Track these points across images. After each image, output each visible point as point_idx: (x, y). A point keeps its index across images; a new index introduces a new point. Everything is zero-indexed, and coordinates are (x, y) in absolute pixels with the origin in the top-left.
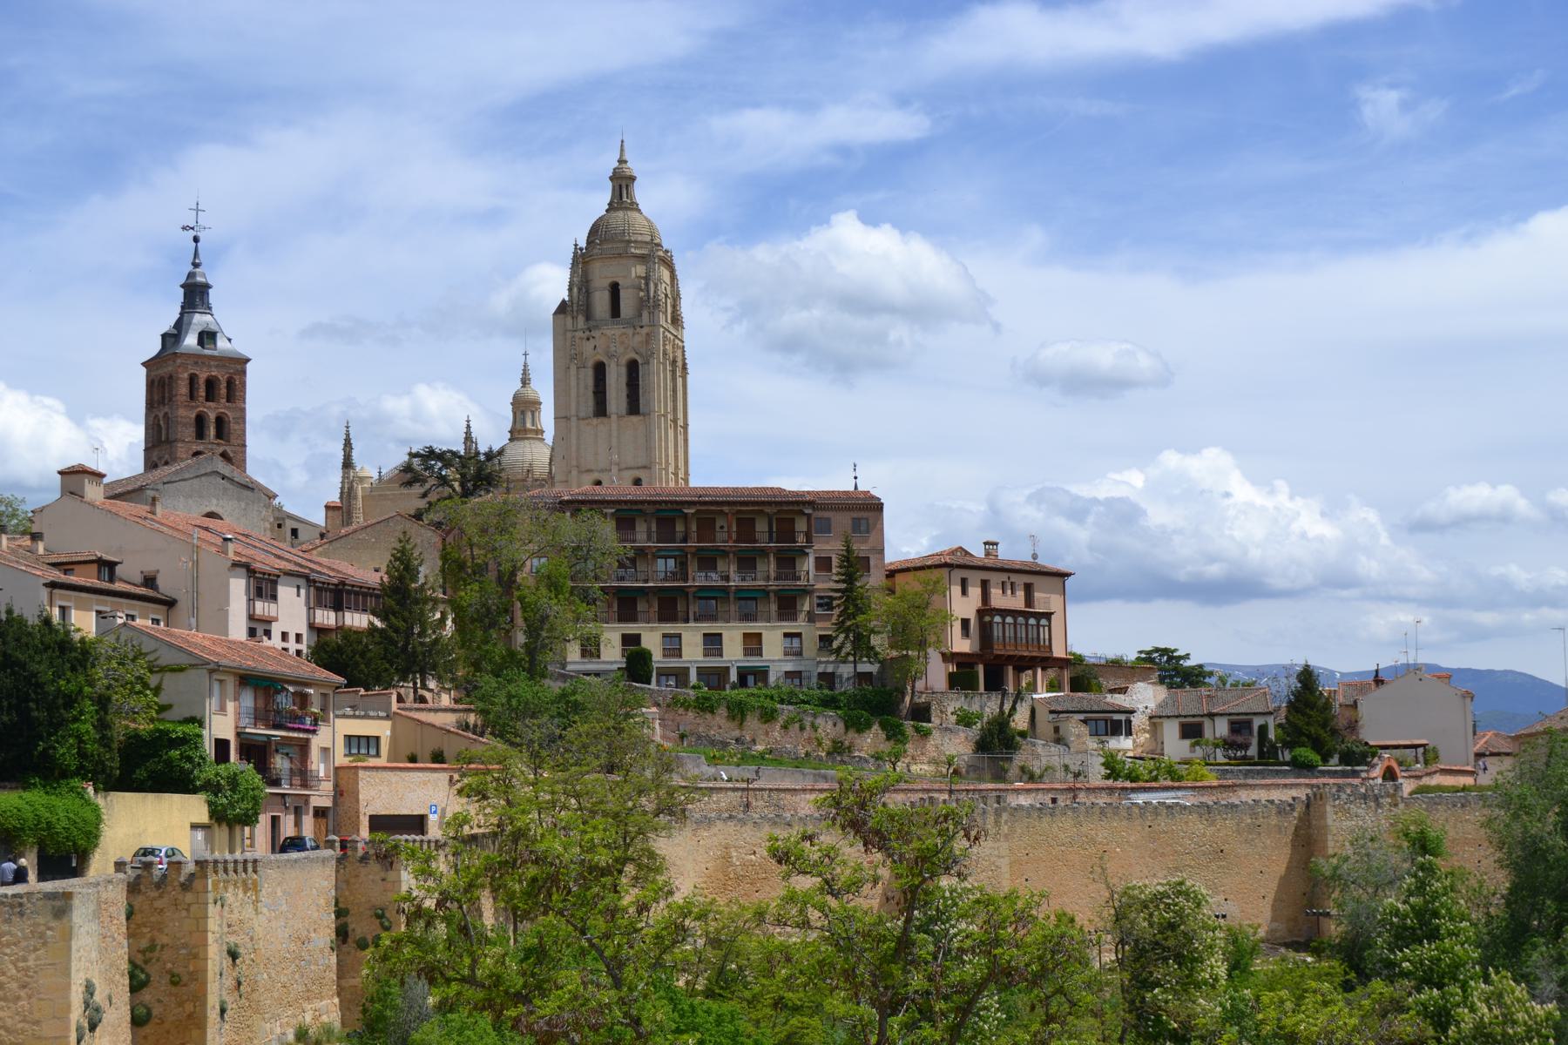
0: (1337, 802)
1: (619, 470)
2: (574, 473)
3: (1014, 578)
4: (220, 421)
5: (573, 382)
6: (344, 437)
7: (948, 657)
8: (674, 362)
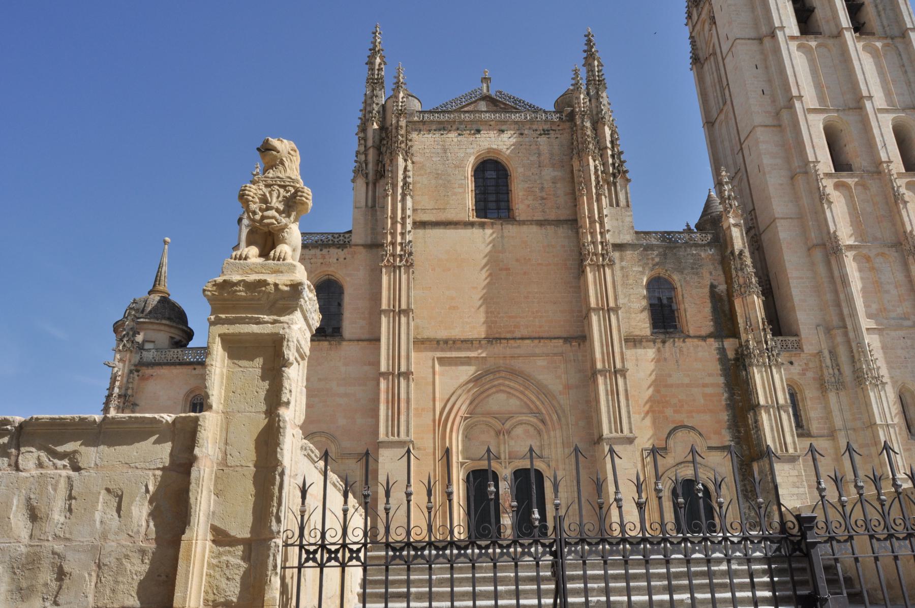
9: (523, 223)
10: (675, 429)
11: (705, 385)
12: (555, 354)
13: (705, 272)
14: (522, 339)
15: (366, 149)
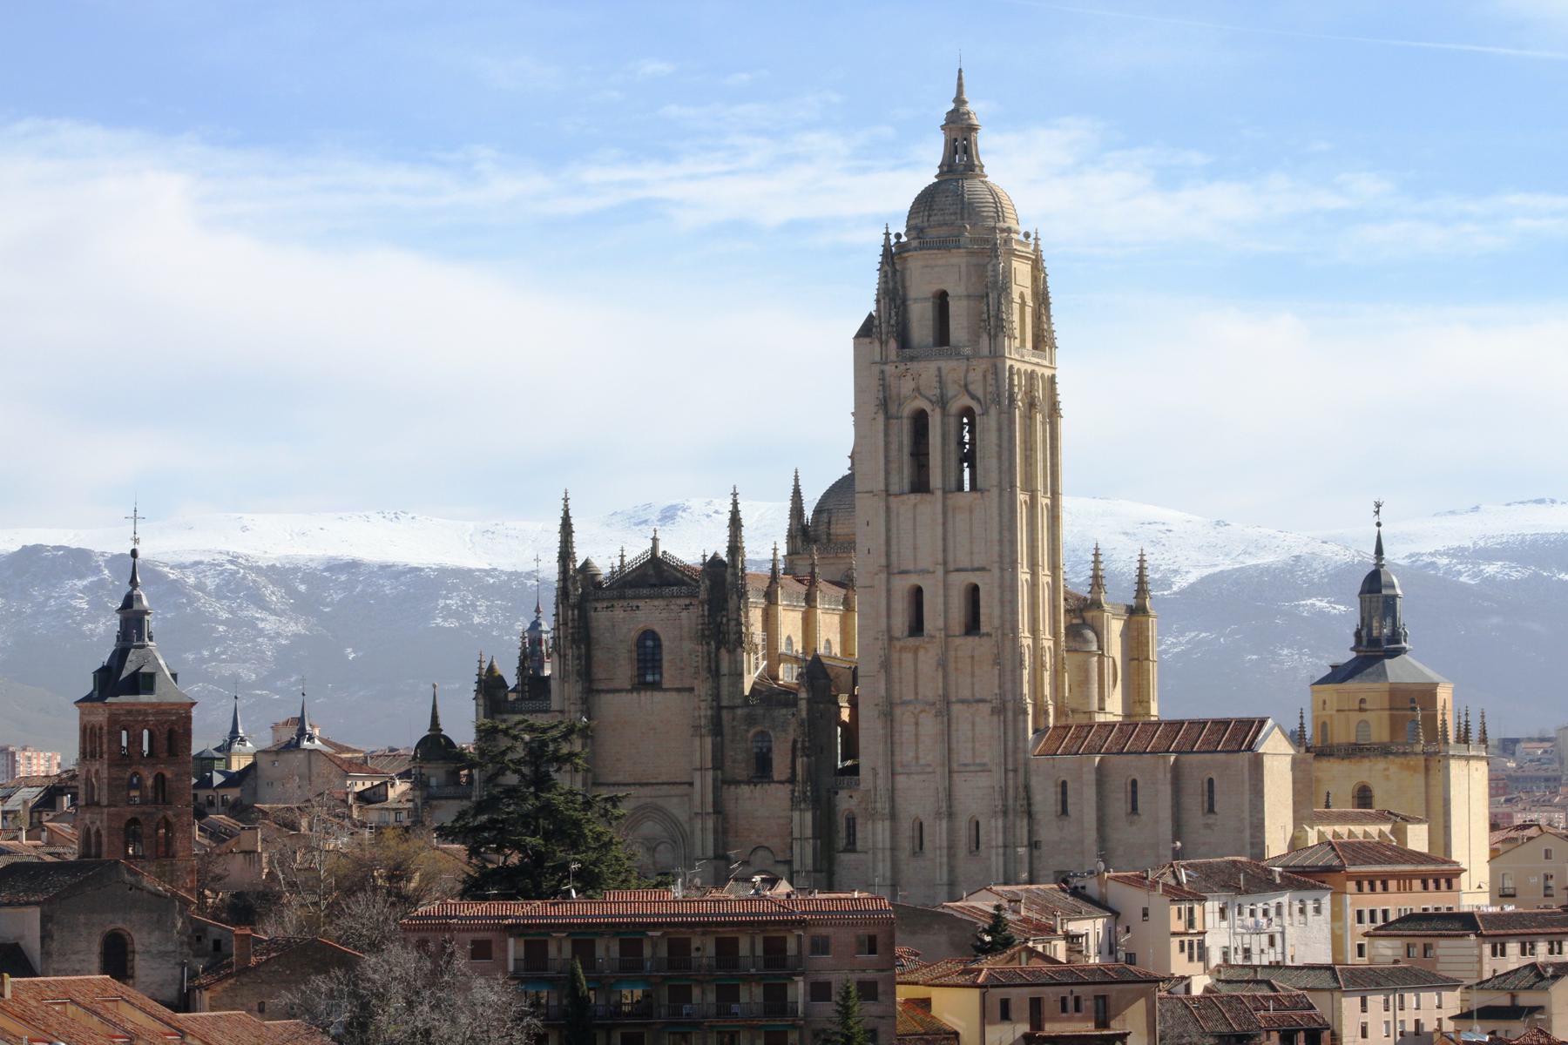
1: (946, 572)
2: (883, 576)
3: (1077, 990)
4: (160, 779)
5: (881, 435)
6: (562, 514)
8: (1032, 405)
10: (755, 849)
11: (779, 817)
12: (682, 796)
13: (791, 730)
14: (663, 784)
15: (559, 625)
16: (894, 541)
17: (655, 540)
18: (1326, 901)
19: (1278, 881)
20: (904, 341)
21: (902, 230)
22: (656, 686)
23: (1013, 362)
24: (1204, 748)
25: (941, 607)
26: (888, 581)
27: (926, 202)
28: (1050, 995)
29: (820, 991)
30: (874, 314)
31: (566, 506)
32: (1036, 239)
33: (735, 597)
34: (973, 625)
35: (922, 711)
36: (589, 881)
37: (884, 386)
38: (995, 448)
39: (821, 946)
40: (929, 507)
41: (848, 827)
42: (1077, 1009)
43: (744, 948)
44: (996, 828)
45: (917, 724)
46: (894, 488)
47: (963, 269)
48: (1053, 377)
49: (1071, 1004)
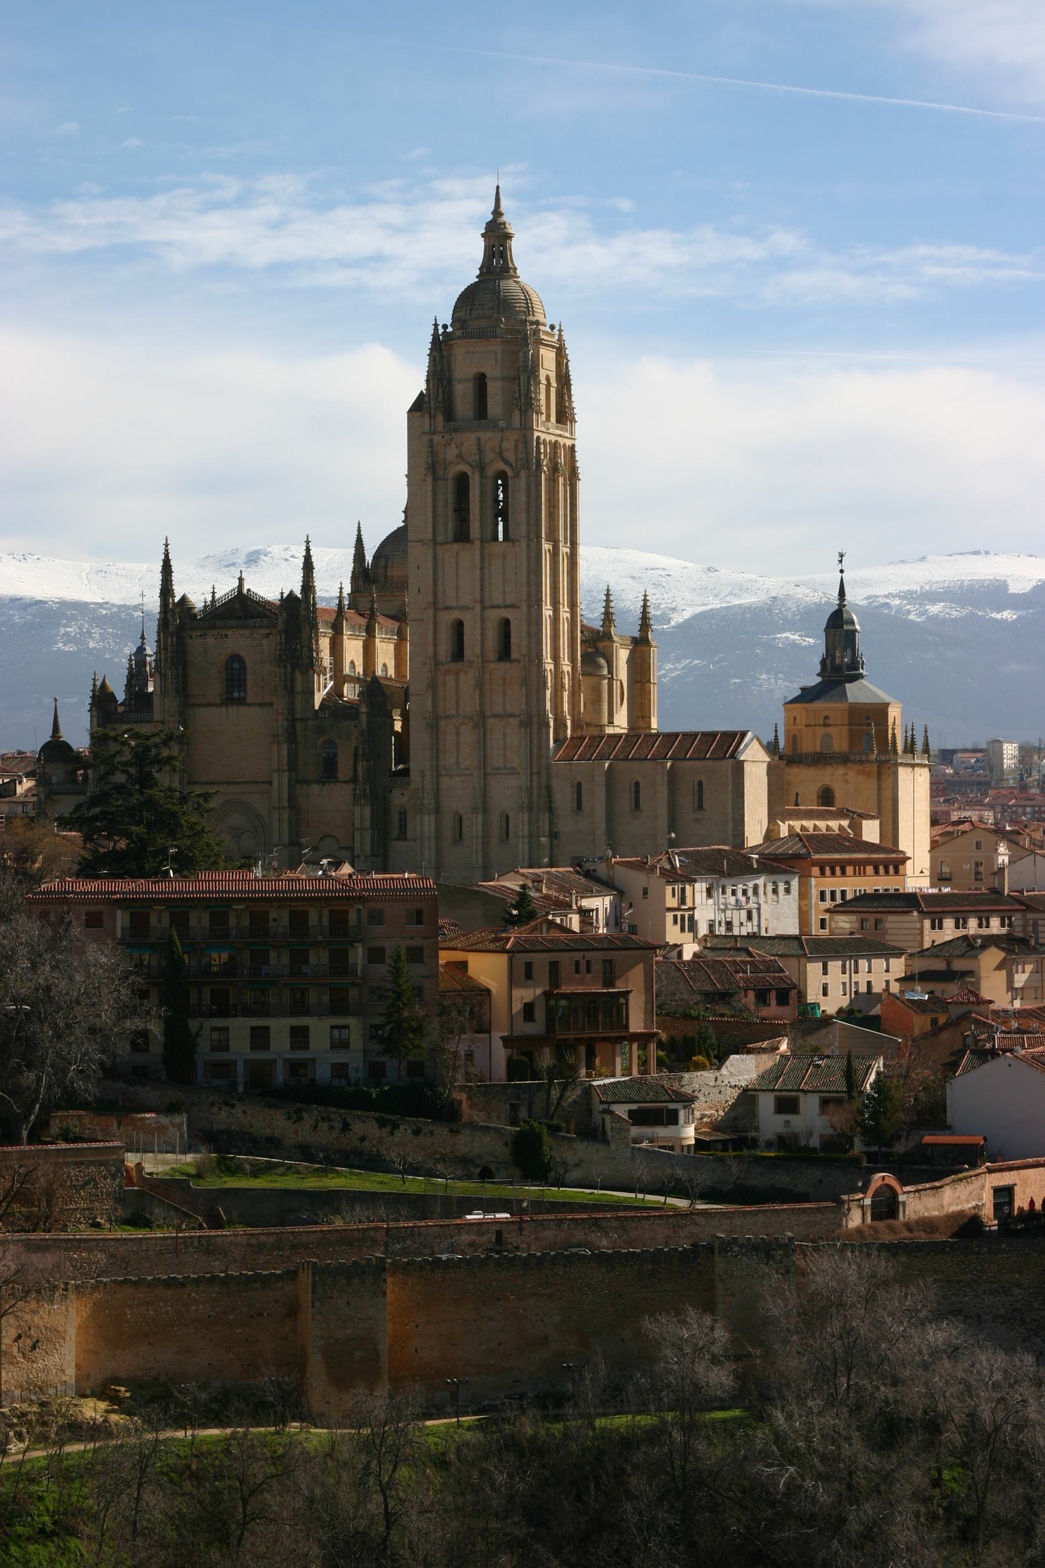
0: (729, 1254)
1: (483, 608)
2: (431, 612)
3: (589, 955)
5: (430, 494)
7: (507, 1041)
8: (555, 469)
9: (250, 705)
10: (323, 838)
14: (247, 782)
15: (160, 649)
16: (440, 583)
17: (241, 580)
18: (795, 883)
19: (755, 866)
20: (449, 415)
21: (449, 322)
22: (241, 701)
23: (540, 434)
24: (695, 756)
25: (479, 638)
26: (435, 616)
27: (468, 300)
28: (566, 959)
29: (376, 955)
30: (424, 392)
31: (167, 550)
32: (560, 330)
33: (307, 627)
34: (505, 653)
35: (463, 724)
36: (185, 864)
37: (432, 452)
38: (524, 506)
39: (376, 918)
40: (469, 556)
41: (400, 819)
42: (588, 971)
43: (313, 919)
44: (523, 821)
45: (458, 734)
46: (441, 538)
47: (499, 355)
48: (573, 446)
49: (583, 966)
